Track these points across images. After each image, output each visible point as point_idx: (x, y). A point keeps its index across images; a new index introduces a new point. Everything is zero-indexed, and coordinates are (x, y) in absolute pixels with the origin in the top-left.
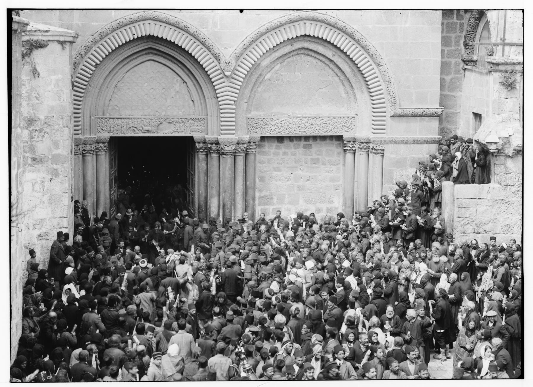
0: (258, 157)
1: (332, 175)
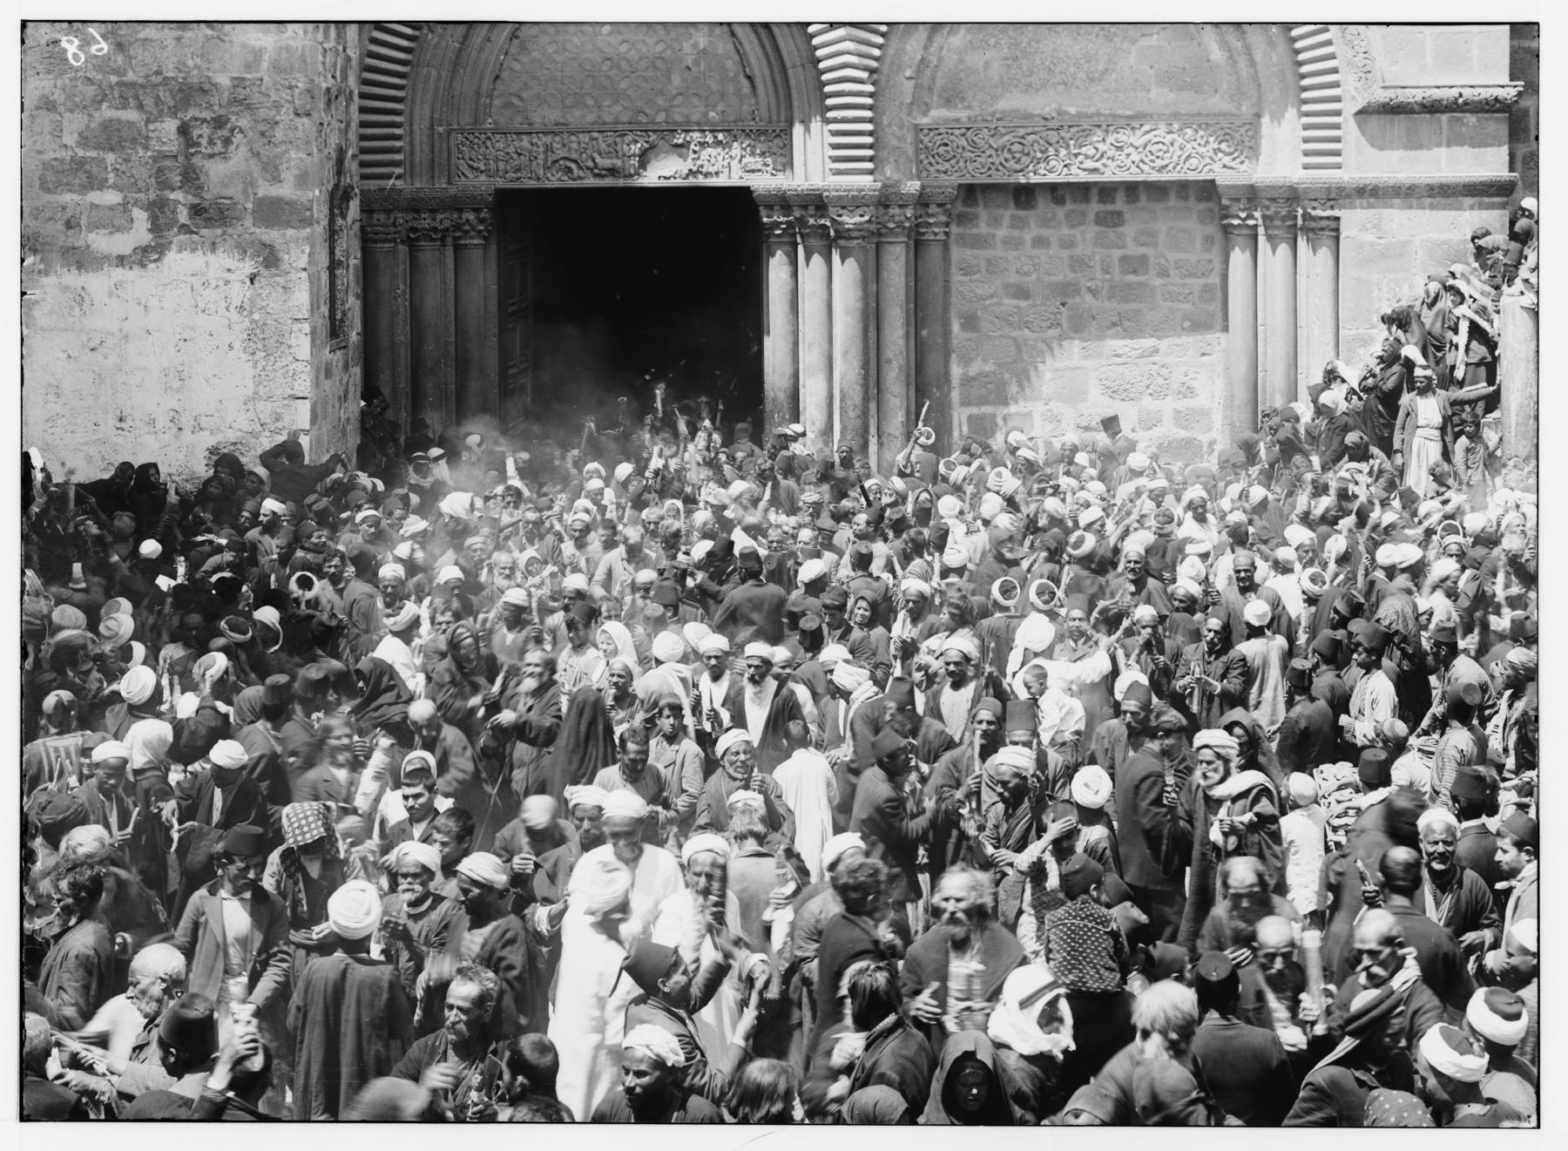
0: (956, 253)
1: (1188, 306)
